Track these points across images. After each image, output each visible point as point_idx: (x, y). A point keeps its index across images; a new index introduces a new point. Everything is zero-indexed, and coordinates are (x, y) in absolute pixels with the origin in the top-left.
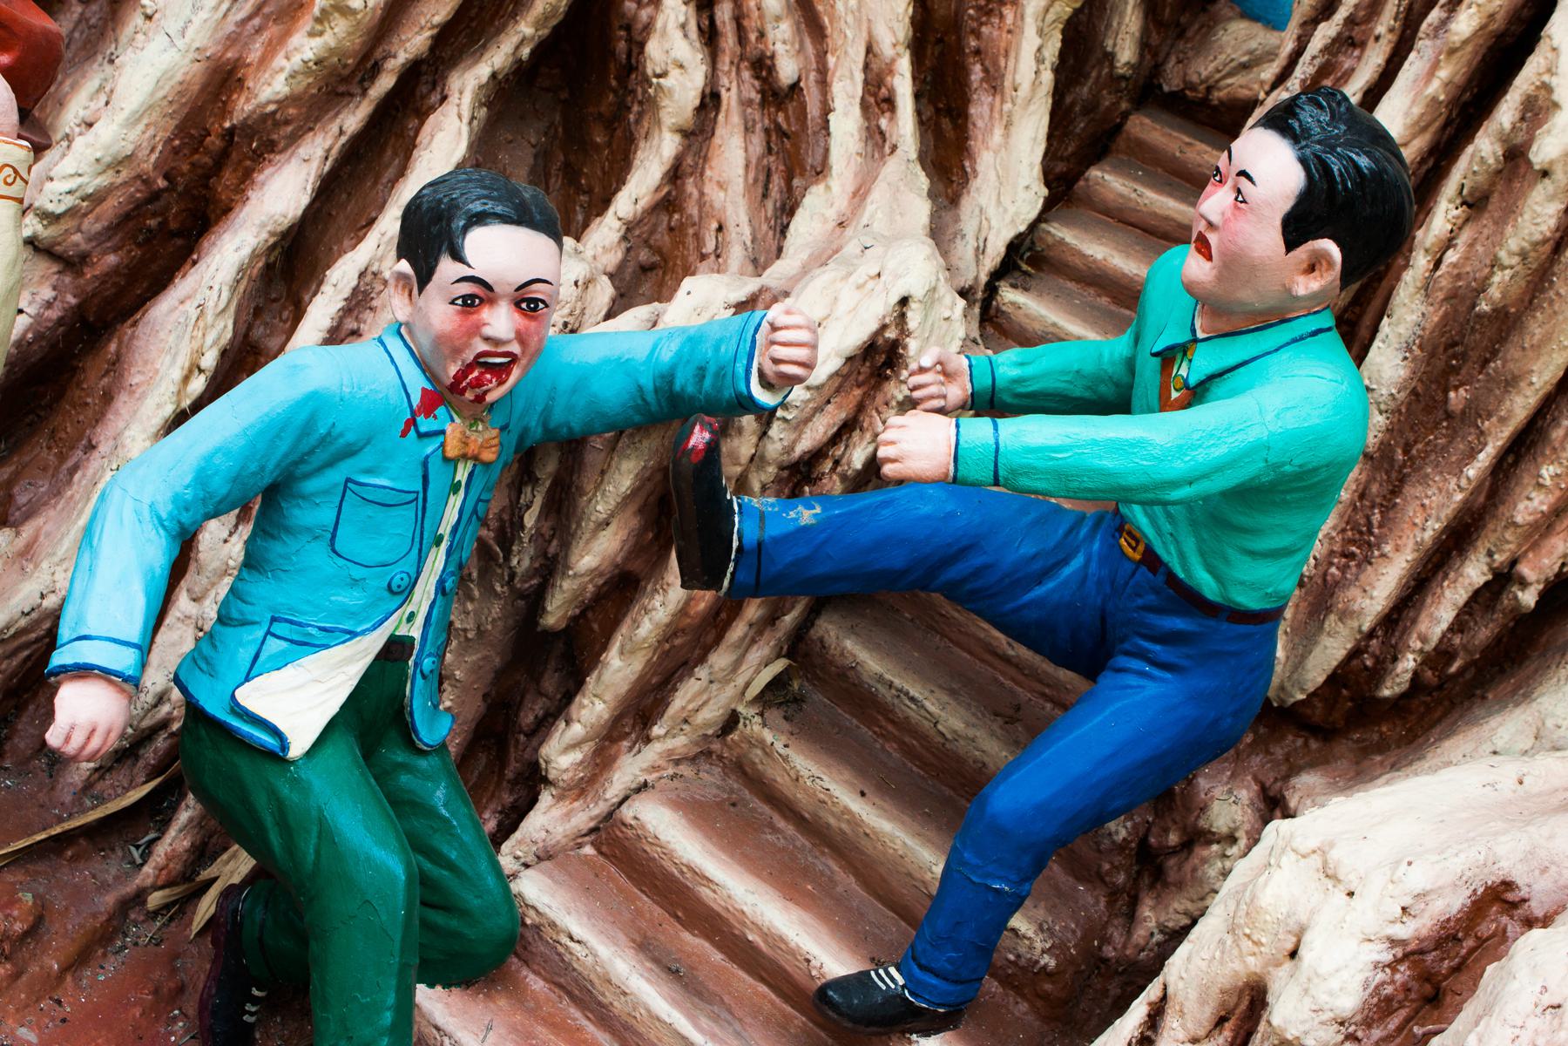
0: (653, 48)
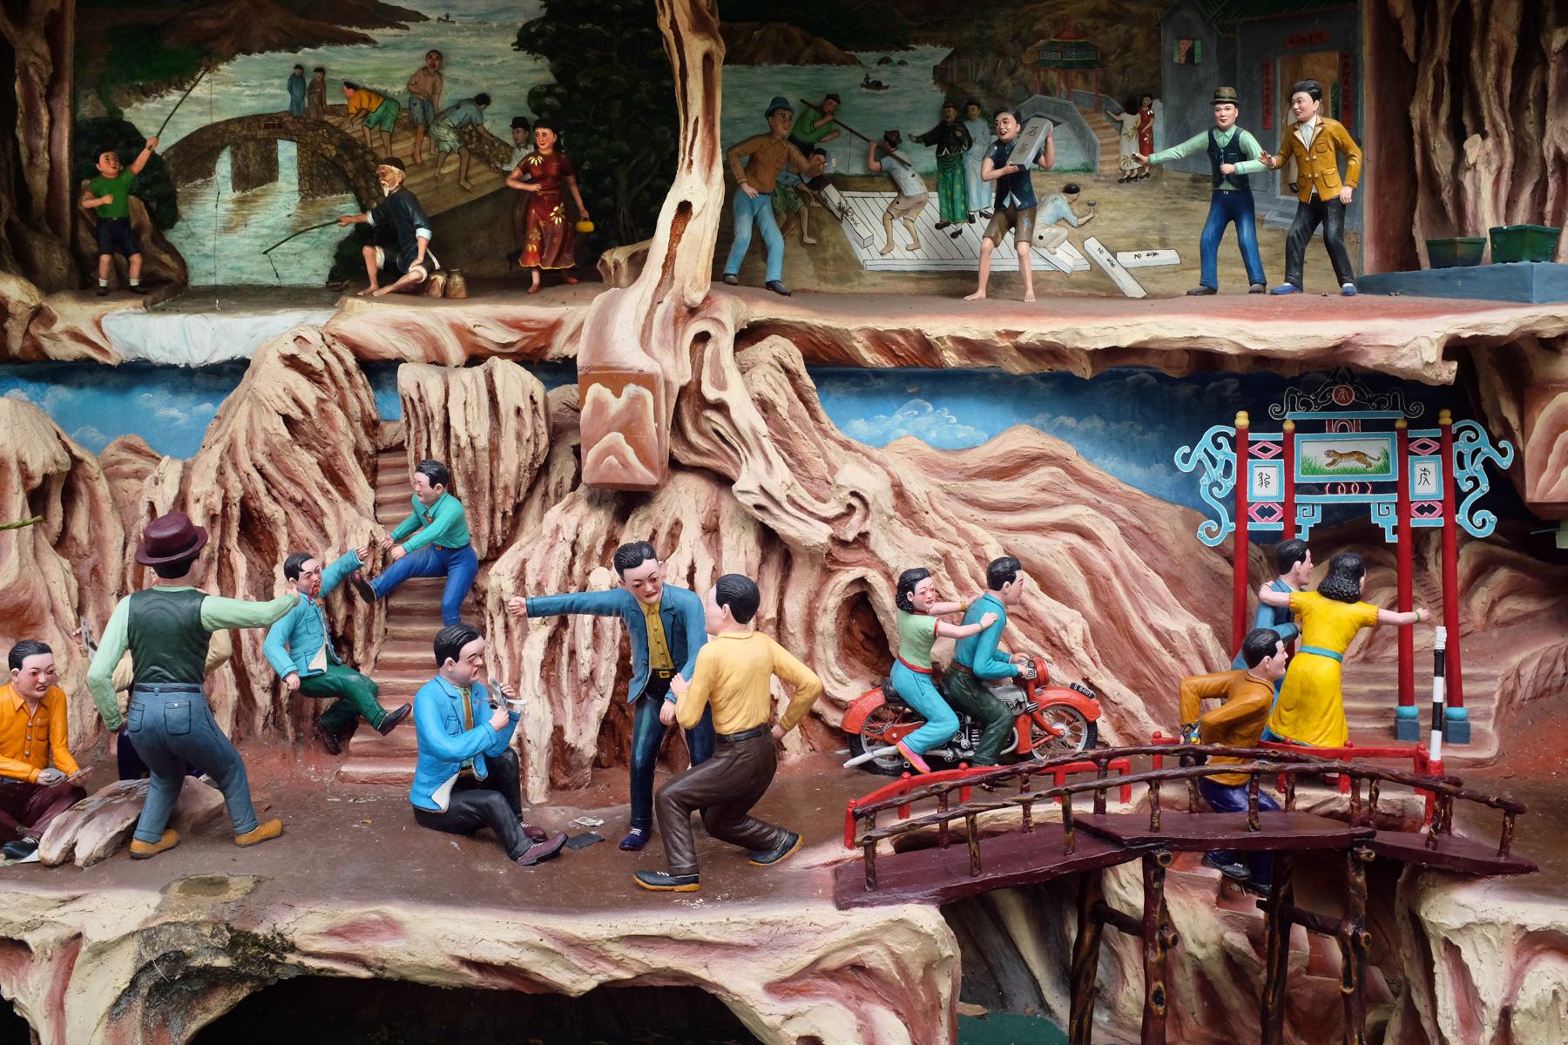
0: (266, 511)
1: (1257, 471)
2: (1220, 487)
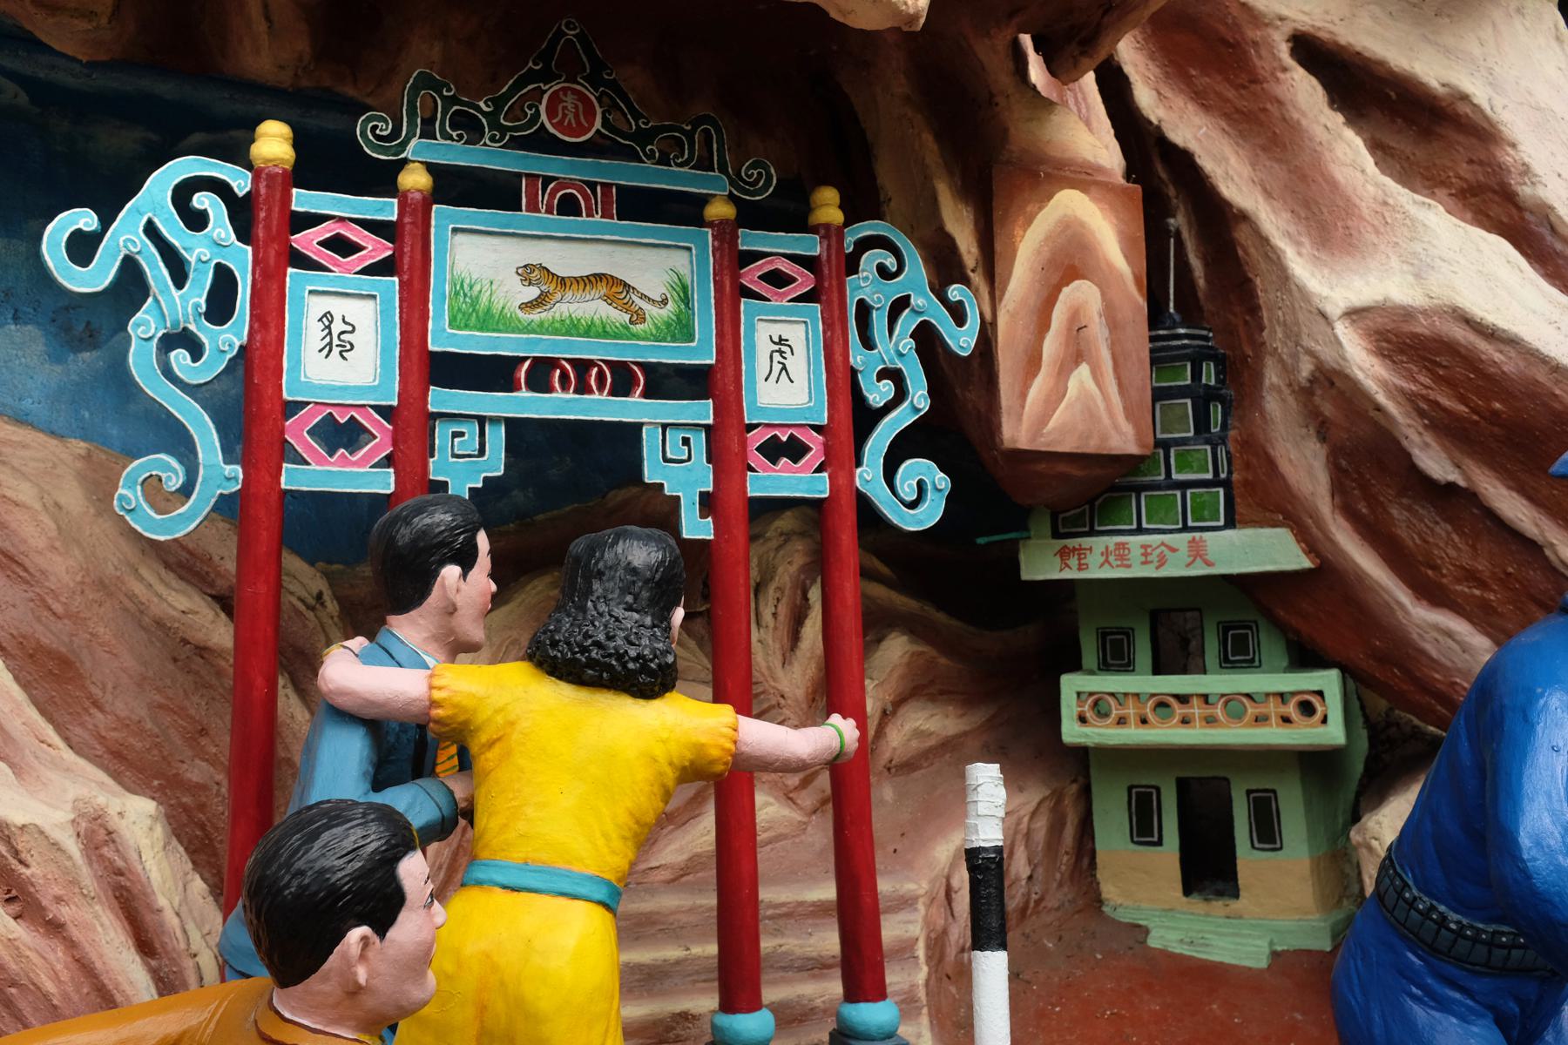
1: (318, 306)
2: (196, 350)
